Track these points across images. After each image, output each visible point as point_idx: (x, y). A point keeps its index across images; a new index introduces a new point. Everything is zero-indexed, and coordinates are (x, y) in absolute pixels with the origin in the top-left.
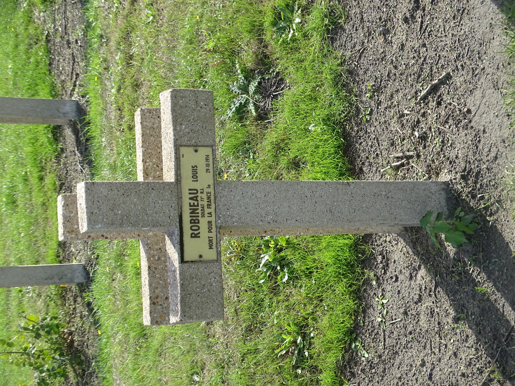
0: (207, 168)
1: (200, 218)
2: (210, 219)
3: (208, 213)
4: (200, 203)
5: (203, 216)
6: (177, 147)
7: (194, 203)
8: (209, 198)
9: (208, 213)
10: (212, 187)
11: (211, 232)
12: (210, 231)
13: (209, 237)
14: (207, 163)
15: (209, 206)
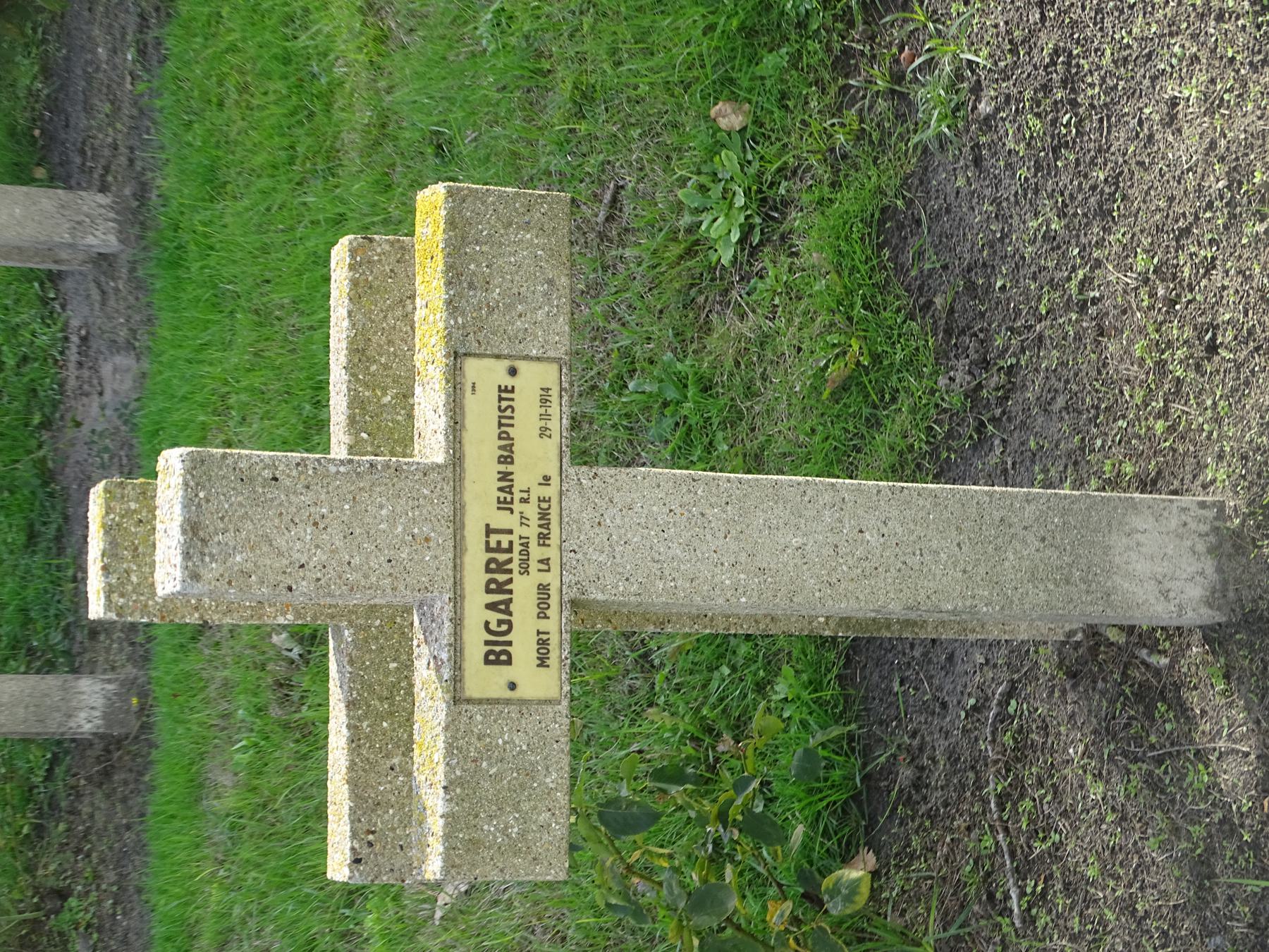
0: (543, 423)
1: (515, 575)
2: (546, 578)
3: (541, 561)
4: (519, 530)
5: (525, 571)
6: (457, 356)
7: (499, 543)
8: (544, 515)
9: (541, 561)
10: (555, 481)
11: (547, 617)
12: (542, 615)
13: (539, 633)
14: (543, 411)
15: (543, 538)
